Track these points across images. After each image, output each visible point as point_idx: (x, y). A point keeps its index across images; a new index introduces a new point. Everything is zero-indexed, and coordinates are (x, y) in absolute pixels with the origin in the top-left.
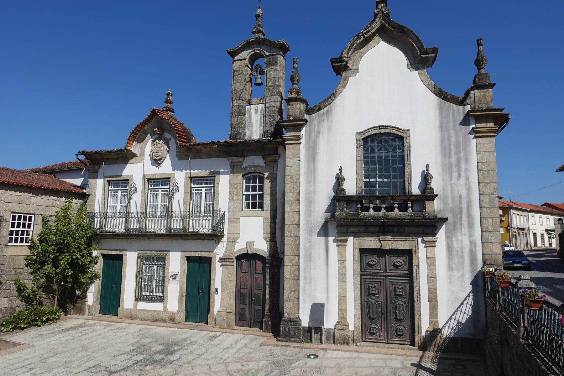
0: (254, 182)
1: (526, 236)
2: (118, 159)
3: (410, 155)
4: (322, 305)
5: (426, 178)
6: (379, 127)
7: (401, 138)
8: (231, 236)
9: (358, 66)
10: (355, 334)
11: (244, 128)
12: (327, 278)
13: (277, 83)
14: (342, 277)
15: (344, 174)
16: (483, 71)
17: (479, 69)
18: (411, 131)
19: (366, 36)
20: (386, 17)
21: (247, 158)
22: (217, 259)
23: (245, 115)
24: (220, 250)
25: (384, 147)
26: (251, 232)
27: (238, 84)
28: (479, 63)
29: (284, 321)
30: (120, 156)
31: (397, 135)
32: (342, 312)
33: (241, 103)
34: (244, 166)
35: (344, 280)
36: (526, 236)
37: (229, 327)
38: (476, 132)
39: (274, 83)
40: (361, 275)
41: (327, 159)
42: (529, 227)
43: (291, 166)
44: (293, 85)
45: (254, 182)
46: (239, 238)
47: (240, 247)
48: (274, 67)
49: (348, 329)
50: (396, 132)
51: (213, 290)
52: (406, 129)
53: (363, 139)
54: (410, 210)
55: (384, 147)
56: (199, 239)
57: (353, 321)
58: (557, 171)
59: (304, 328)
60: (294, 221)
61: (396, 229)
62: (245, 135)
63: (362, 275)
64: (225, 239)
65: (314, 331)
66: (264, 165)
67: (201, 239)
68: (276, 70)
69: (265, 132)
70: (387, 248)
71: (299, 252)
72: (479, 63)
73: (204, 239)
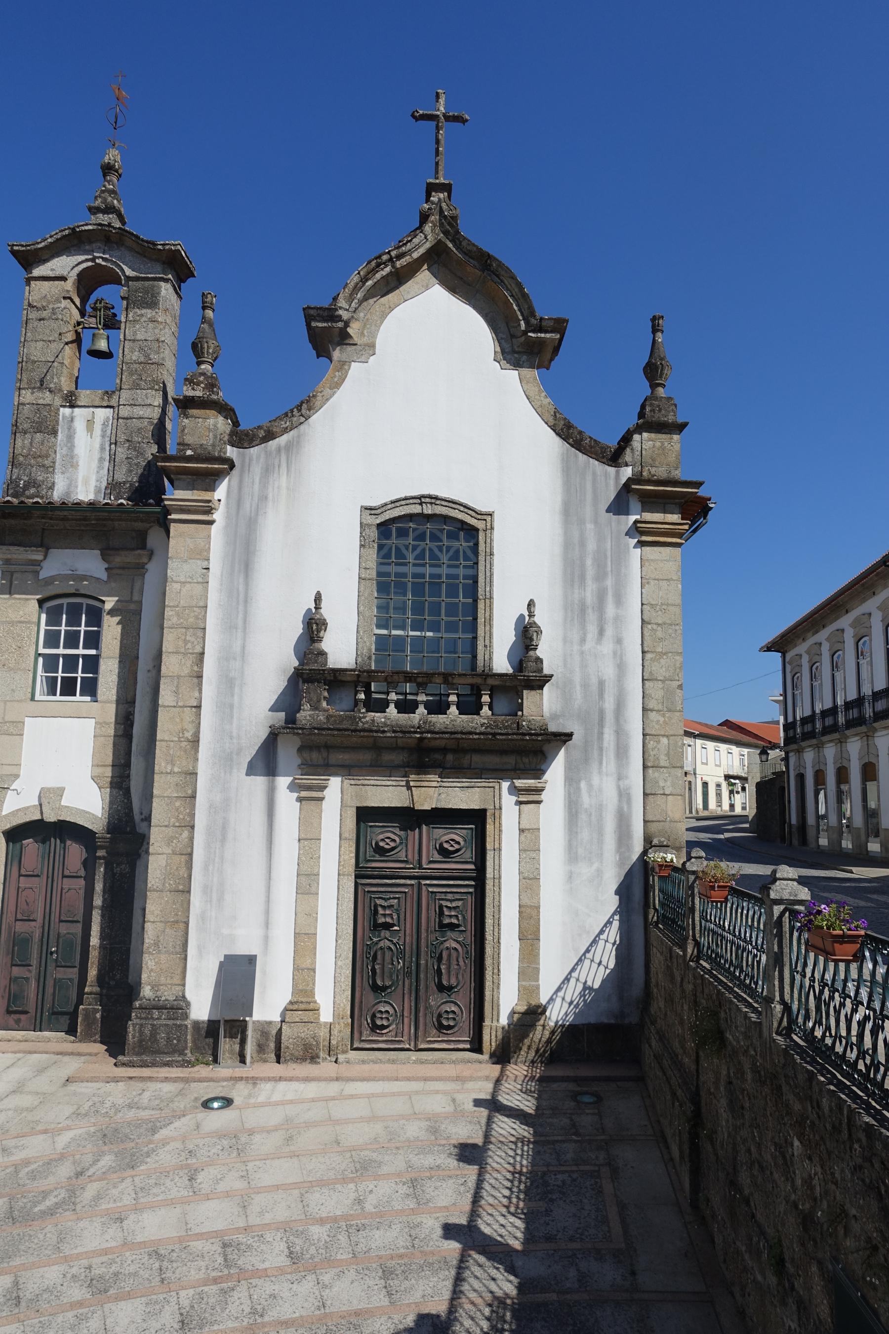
0: (74, 620)
1: (690, 789)
3: (491, 575)
4: (251, 960)
5: (527, 634)
6: (420, 499)
7: (472, 532)
9: (374, 336)
10: (335, 1032)
11: (50, 469)
12: (263, 888)
13: (154, 357)
15: (326, 612)
16: (661, 391)
17: (654, 386)
18: (496, 516)
19: (398, 264)
20: (449, 225)
23: (54, 433)
25: (428, 551)
27: (40, 344)
28: (653, 372)
29: (141, 1008)
31: (463, 522)
32: (304, 974)
33: (46, 398)
34: (43, 574)
35: (313, 890)
36: (690, 789)
38: (642, 533)
39: (147, 356)
40: (357, 877)
41: (280, 570)
42: (695, 770)
43: (183, 583)
44: (199, 364)
45: (74, 620)
46: (17, 776)
48: (149, 313)
49: (316, 1022)
50: (460, 516)
52: (484, 509)
53: (379, 525)
54: (485, 711)
55: (428, 551)
57: (330, 997)
59: (196, 1024)
60: (183, 730)
61: (450, 757)
62: (52, 487)
63: (360, 874)
65: (227, 1030)
66: (104, 576)
68: (153, 320)
69: (113, 486)
70: (427, 807)
71: (192, 816)
72: (653, 372)
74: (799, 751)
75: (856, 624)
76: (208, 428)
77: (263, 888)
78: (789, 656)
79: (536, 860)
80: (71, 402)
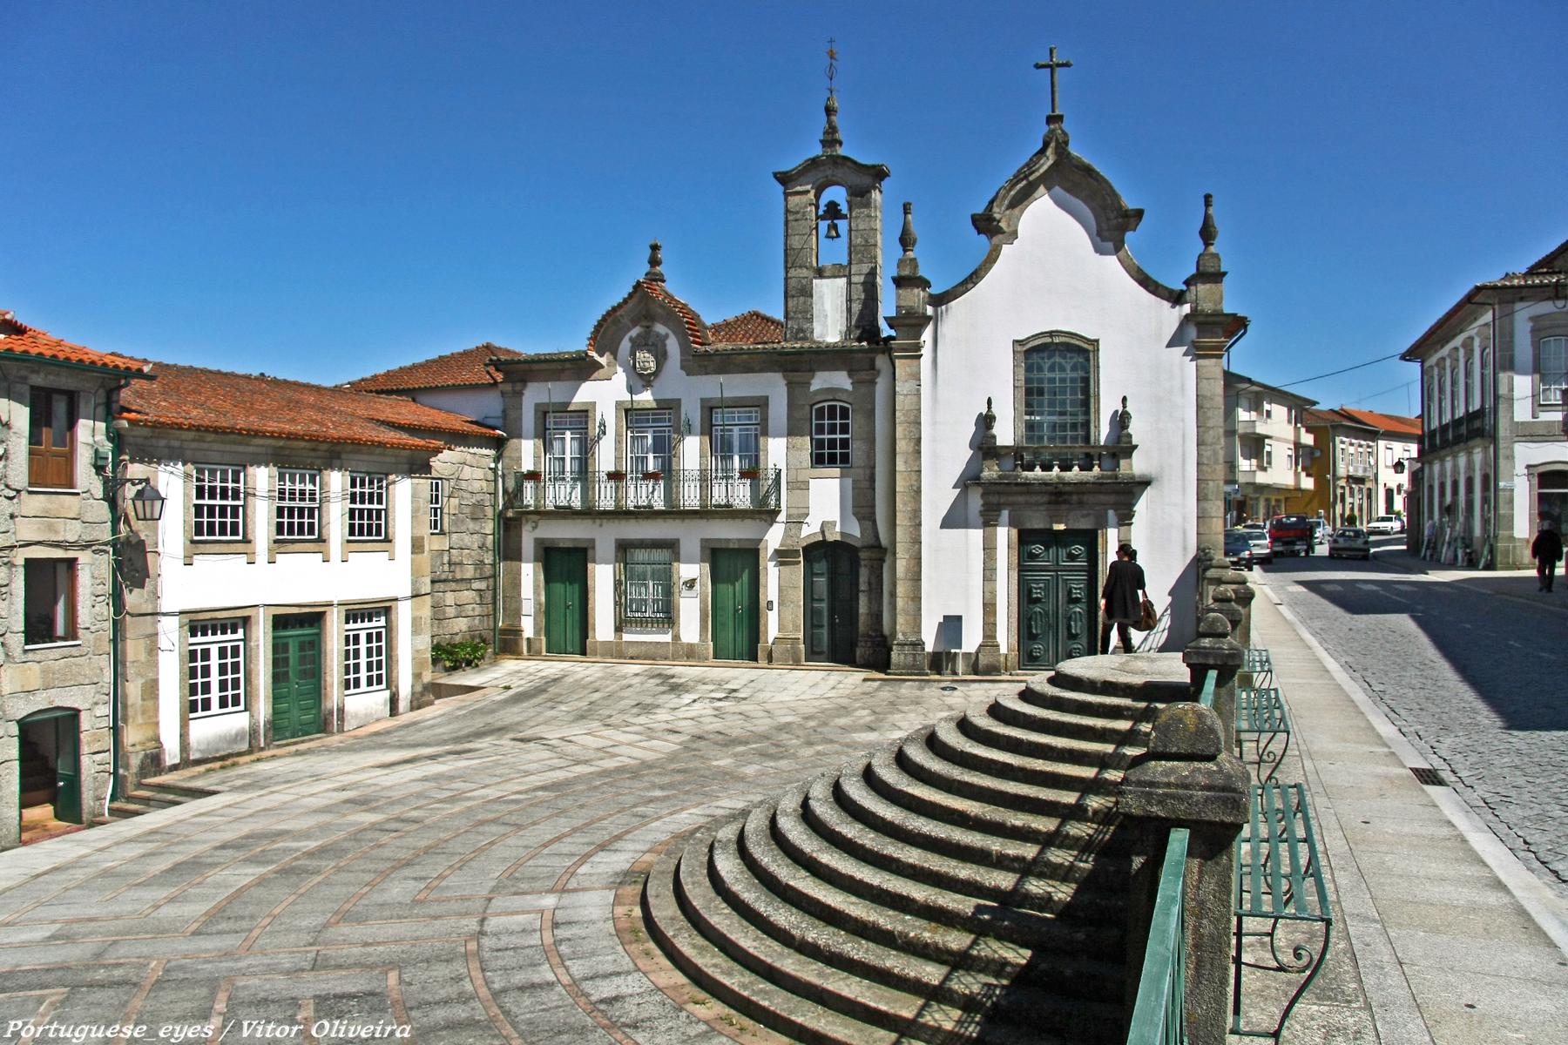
1: (1369, 497)
2: (563, 370)
4: (959, 618)
6: (1051, 334)
8: (793, 511)
11: (811, 320)
12: (959, 578)
16: (1212, 249)
17: (1207, 244)
21: (819, 374)
22: (770, 552)
24: (774, 538)
25: (1057, 368)
26: (824, 504)
33: (804, 272)
34: (813, 388)
36: (1369, 497)
37: (797, 662)
38: (1198, 348)
42: (1376, 475)
47: (810, 530)
48: (866, 211)
51: (763, 604)
54: (1096, 468)
55: (1057, 368)
57: (1005, 639)
61: (1075, 497)
63: (1022, 569)
64: (782, 517)
66: (850, 388)
69: (849, 330)
72: (1207, 234)
74: (1431, 463)
75: (1464, 345)
76: (916, 297)
77: (959, 578)
78: (1427, 365)
80: (820, 273)
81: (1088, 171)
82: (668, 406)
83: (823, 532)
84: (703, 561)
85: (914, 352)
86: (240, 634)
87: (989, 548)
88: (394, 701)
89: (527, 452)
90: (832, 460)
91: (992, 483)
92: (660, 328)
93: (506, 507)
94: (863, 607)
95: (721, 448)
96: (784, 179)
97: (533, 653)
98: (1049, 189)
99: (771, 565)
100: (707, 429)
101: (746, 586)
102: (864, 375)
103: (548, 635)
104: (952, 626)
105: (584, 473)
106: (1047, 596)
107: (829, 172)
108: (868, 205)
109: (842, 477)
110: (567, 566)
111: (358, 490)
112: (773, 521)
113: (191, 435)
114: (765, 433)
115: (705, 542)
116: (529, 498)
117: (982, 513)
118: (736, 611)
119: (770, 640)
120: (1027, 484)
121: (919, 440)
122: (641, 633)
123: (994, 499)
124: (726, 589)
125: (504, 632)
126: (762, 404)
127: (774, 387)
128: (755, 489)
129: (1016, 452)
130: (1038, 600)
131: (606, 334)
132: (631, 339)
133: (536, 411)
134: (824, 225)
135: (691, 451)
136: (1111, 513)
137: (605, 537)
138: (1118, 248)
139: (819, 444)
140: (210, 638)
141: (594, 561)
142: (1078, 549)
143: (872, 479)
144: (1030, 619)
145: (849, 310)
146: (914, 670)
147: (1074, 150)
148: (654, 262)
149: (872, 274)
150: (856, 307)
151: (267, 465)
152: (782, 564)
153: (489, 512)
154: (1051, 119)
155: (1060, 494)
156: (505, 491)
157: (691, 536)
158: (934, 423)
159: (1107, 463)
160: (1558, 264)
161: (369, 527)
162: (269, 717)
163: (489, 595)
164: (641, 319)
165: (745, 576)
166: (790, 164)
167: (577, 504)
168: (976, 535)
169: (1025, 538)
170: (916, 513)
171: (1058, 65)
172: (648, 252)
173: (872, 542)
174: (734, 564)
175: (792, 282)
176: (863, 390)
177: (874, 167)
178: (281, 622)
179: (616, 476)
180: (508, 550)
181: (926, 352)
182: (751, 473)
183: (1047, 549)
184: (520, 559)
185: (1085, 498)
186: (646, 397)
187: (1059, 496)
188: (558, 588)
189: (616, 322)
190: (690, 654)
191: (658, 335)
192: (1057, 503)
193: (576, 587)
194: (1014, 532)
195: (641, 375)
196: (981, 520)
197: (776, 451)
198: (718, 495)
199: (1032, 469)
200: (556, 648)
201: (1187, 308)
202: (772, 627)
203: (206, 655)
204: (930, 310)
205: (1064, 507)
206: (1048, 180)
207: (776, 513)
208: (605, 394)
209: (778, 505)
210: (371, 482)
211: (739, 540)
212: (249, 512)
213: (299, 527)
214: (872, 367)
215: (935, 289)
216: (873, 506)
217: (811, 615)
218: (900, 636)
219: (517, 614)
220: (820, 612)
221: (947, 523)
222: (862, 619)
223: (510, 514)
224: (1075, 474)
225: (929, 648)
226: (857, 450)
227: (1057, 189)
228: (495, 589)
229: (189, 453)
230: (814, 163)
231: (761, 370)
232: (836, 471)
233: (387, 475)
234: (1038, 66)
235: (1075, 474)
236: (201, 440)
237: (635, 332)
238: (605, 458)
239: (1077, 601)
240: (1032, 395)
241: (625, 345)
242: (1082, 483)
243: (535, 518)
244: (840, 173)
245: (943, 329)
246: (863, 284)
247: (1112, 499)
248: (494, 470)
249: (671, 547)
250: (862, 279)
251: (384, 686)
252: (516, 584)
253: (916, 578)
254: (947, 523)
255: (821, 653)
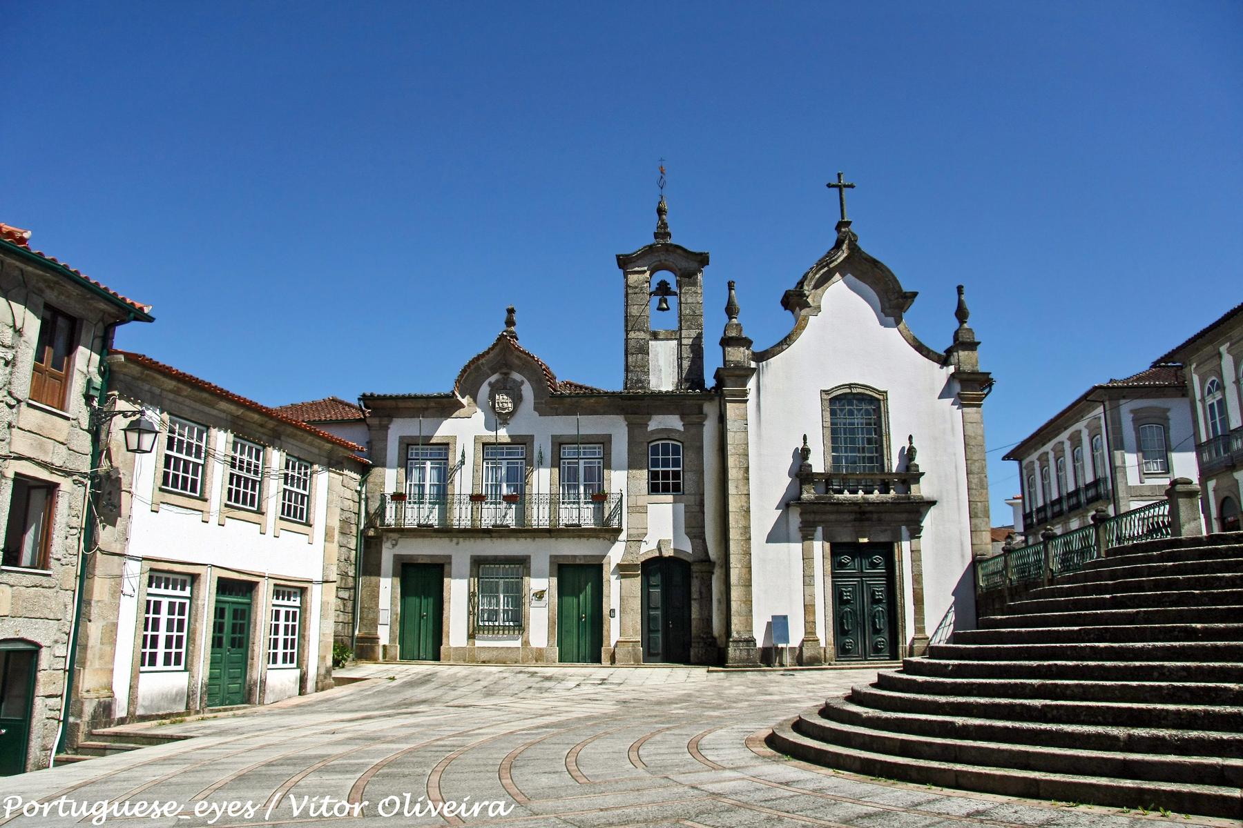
2: (426, 409)
4: (785, 617)
6: (850, 386)
7: (872, 400)
12: (783, 584)
14: (808, 580)
15: (809, 445)
16: (966, 325)
20: (854, 248)
22: (613, 566)
24: (616, 554)
25: (856, 412)
26: (658, 526)
28: (961, 314)
30: (432, 404)
33: (642, 335)
34: (649, 429)
38: (962, 399)
41: (779, 426)
44: (730, 318)
47: (648, 549)
48: (693, 289)
51: (606, 611)
55: (856, 412)
56: (580, 537)
58: (1004, 459)
61: (875, 516)
63: (834, 576)
64: (623, 536)
65: (769, 657)
66: (682, 429)
67: (584, 536)
69: (680, 382)
72: (961, 314)
73: (589, 537)
75: (1070, 438)
76: (738, 354)
77: (783, 584)
78: (1024, 463)
79: (920, 566)
80: (655, 336)
81: (875, 263)
82: (522, 442)
83: (659, 549)
84: (551, 575)
85: (742, 398)
86: (187, 593)
87: (807, 558)
88: (303, 680)
89: (390, 479)
90: (666, 490)
91: (811, 503)
92: (516, 376)
93: (368, 526)
94: (695, 614)
95: (569, 479)
96: (625, 262)
97: (388, 658)
98: (843, 275)
99: (613, 578)
100: (556, 462)
101: (589, 596)
102: (694, 419)
103: (402, 643)
104: (779, 625)
105: (442, 497)
106: (855, 598)
107: (662, 257)
108: (695, 284)
109: (675, 502)
110: (423, 581)
111: (290, 473)
112: (616, 540)
113: (171, 384)
114: (608, 466)
115: (553, 558)
116: (390, 518)
117: (801, 529)
118: (579, 619)
119: (613, 644)
120: (840, 504)
121: (747, 469)
122: (493, 639)
123: (811, 518)
124: (571, 601)
125: (361, 639)
126: (605, 442)
127: (617, 428)
128: (599, 512)
129: (827, 480)
130: (848, 602)
131: (469, 380)
132: (490, 384)
133: (400, 443)
134: (656, 299)
135: (542, 480)
136: (904, 528)
137: (461, 554)
138: (898, 322)
139: (654, 476)
140: (162, 591)
141: (450, 576)
142: (877, 559)
143: (702, 504)
144: (842, 618)
145: (680, 366)
146: (747, 664)
147: (865, 246)
148: (510, 323)
149: (699, 337)
150: (686, 364)
151: (226, 431)
152: (623, 577)
153: (354, 528)
154: (839, 226)
155: (864, 513)
156: (367, 512)
157: (541, 553)
158: (759, 455)
159: (900, 487)
160: (1177, 357)
161: (296, 511)
162: (206, 680)
163: (350, 604)
164: (501, 367)
165: (589, 588)
166: (632, 248)
167: (434, 520)
168: (797, 548)
169: (837, 550)
170: (746, 530)
171: (845, 186)
172: (506, 314)
173: (702, 557)
174: (579, 579)
175: (632, 343)
176: (693, 431)
177: (701, 254)
178: (225, 586)
179: (476, 498)
180: (368, 564)
181: (752, 396)
182: (599, 498)
183: (853, 560)
184: (379, 575)
185: (883, 516)
186: (503, 434)
187: (862, 513)
188: (413, 601)
189: (478, 368)
190: (539, 656)
191: (514, 381)
192: (861, 520)
193: (431, 600)
194: (827, 545)
195: (499, 414)
196: (799, 535)
197: (617, 481)
198: (567, 515)
199: (841, 492)
200: (407, 655)
201: (952, 369)
202: (614, 632)
203: (158, 605)
204: (753, 365)
205: (866, 523)
206: (843, 269)
207: (619, 530)
208: (466, 430)
209: (620, 524)
210: (300, 469)
211: (585, 556)
212: (209, 471)
213: (244, 495)
214: (700, 411)
215: (757, 348)
216: (704, 527)
217: (647, 621)
218: (735, 635)
219: (374, 623)
220: (655, 618)
221: (772, 538)
222: (694, 623)
223: (371, 533)
224: (876, 495)
225: (760, 644)
226: (688, 482)
227: (849, 276)
228: (355, 601)
229: (167, 402)
230: (650, 249)
231: (604, 413)
232: (670, 498)
233: (312, 464)
234: (829, 186)
235: (876, 495)
236: (177, 392)
237: (493, 378)
238: (463, 483)
239: (879, 602)
240: (837, 435)
241: (485, 390)
242: (883, 503)
243: (395, 536)
244: (670, 259)
245: (765, 380)
246: (692, 346)
247: (904, 516)
248: (359, 493)
249: (522, 564)
250: (690, 341)
251: (294, 665)
252: (375, 596)
253: (748, 584)
254: (772, 538)
255: (658, 654)
